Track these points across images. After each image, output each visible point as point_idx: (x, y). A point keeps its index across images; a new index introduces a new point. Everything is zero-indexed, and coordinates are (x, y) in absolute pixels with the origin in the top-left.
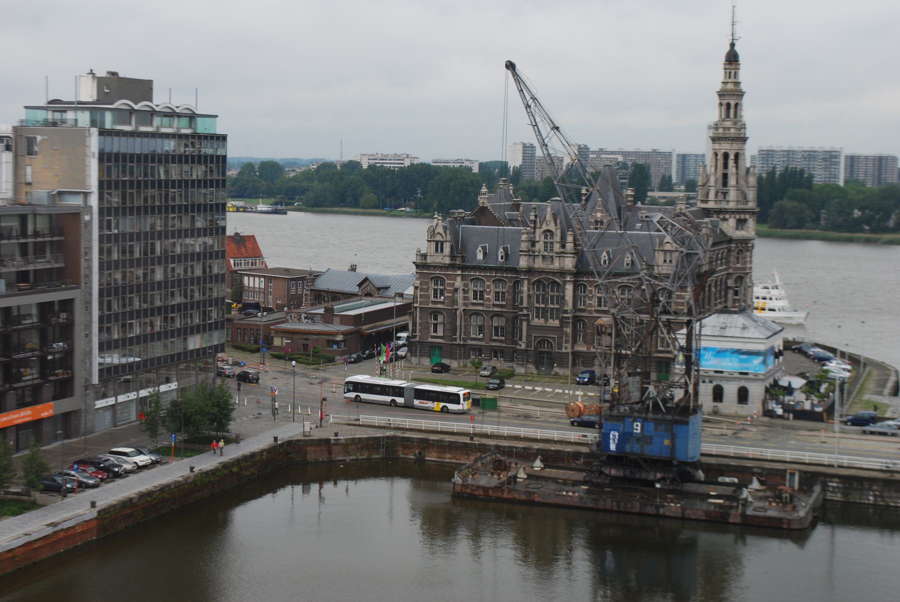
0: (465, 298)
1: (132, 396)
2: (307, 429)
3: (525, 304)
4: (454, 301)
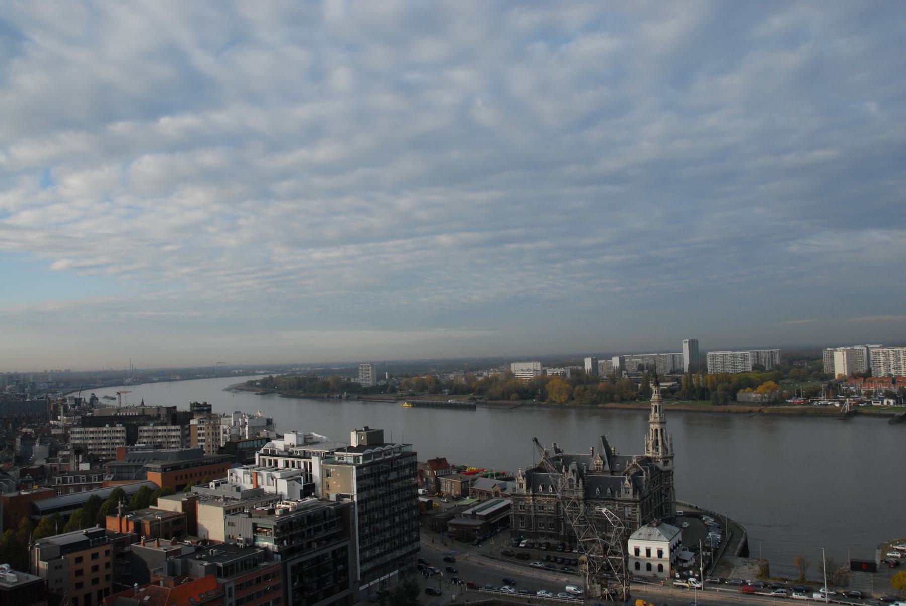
0: (535, 510)
1: (377, 581)
2: (454, 599)
3: (562, 514)
4: (530, 512)
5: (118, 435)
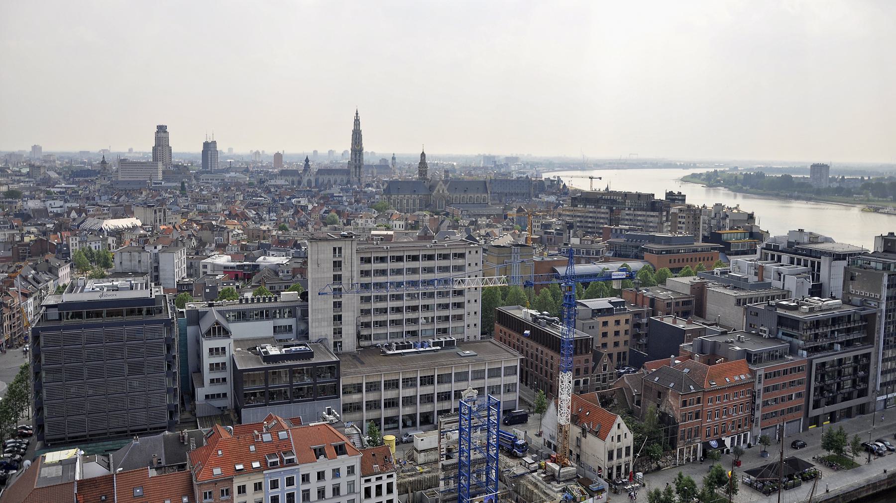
5: (603, 216)
